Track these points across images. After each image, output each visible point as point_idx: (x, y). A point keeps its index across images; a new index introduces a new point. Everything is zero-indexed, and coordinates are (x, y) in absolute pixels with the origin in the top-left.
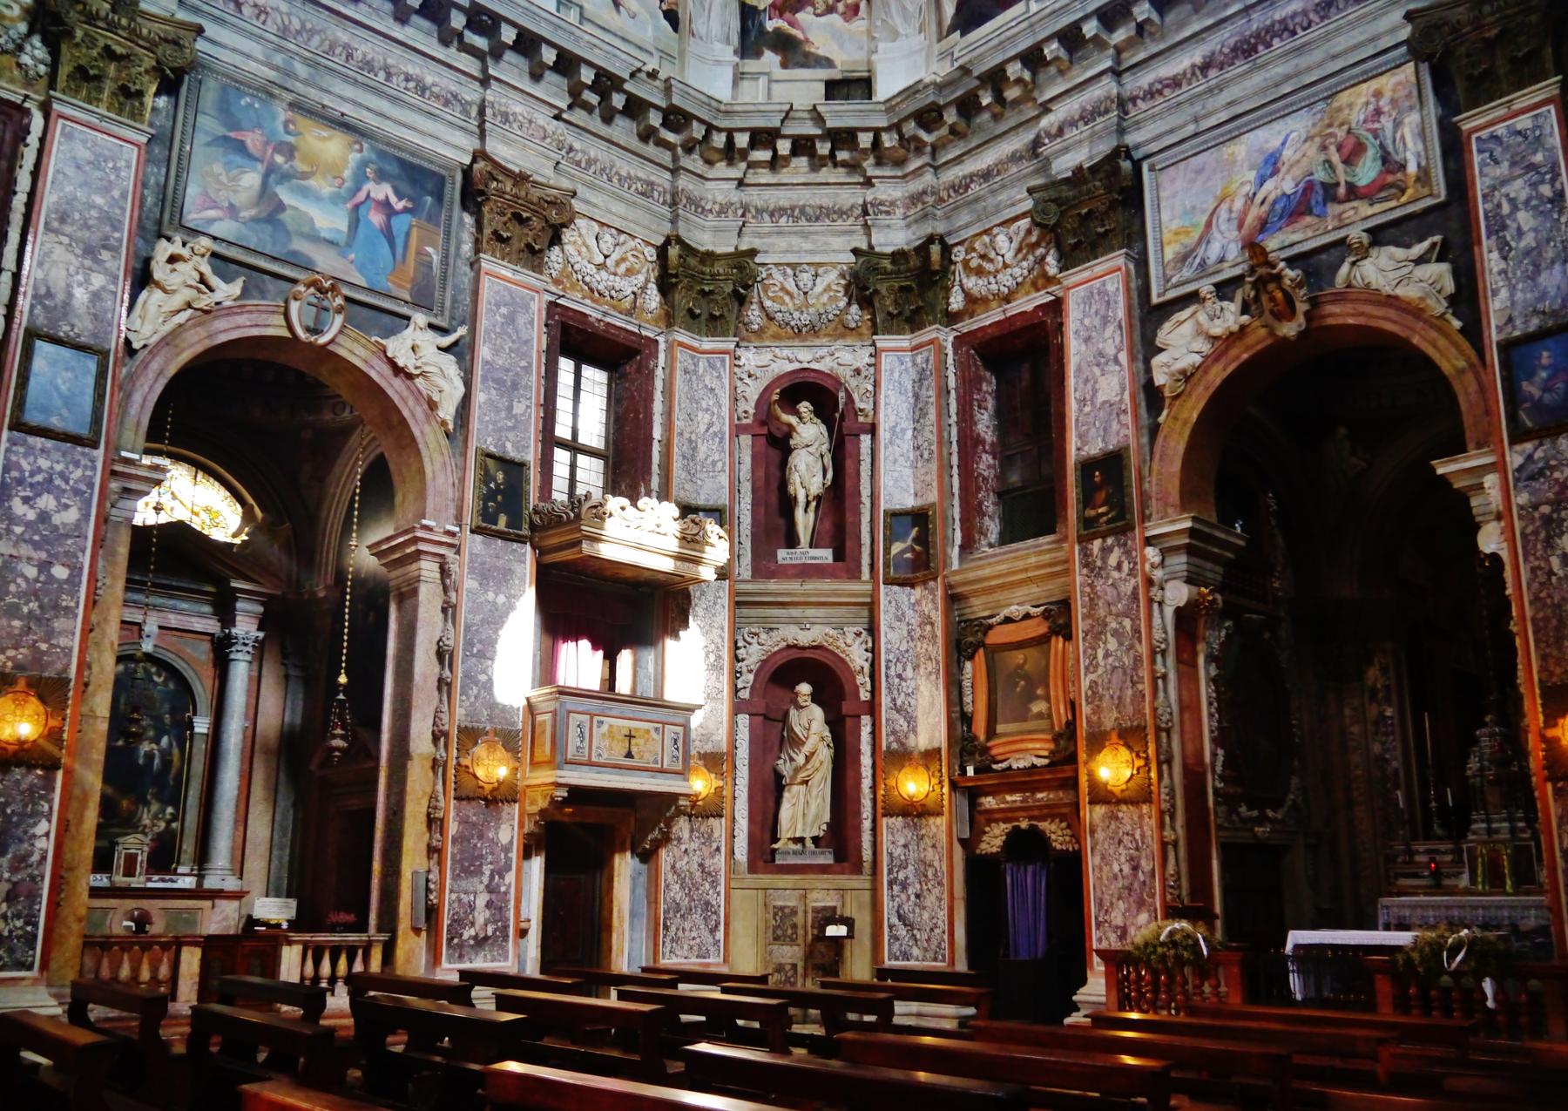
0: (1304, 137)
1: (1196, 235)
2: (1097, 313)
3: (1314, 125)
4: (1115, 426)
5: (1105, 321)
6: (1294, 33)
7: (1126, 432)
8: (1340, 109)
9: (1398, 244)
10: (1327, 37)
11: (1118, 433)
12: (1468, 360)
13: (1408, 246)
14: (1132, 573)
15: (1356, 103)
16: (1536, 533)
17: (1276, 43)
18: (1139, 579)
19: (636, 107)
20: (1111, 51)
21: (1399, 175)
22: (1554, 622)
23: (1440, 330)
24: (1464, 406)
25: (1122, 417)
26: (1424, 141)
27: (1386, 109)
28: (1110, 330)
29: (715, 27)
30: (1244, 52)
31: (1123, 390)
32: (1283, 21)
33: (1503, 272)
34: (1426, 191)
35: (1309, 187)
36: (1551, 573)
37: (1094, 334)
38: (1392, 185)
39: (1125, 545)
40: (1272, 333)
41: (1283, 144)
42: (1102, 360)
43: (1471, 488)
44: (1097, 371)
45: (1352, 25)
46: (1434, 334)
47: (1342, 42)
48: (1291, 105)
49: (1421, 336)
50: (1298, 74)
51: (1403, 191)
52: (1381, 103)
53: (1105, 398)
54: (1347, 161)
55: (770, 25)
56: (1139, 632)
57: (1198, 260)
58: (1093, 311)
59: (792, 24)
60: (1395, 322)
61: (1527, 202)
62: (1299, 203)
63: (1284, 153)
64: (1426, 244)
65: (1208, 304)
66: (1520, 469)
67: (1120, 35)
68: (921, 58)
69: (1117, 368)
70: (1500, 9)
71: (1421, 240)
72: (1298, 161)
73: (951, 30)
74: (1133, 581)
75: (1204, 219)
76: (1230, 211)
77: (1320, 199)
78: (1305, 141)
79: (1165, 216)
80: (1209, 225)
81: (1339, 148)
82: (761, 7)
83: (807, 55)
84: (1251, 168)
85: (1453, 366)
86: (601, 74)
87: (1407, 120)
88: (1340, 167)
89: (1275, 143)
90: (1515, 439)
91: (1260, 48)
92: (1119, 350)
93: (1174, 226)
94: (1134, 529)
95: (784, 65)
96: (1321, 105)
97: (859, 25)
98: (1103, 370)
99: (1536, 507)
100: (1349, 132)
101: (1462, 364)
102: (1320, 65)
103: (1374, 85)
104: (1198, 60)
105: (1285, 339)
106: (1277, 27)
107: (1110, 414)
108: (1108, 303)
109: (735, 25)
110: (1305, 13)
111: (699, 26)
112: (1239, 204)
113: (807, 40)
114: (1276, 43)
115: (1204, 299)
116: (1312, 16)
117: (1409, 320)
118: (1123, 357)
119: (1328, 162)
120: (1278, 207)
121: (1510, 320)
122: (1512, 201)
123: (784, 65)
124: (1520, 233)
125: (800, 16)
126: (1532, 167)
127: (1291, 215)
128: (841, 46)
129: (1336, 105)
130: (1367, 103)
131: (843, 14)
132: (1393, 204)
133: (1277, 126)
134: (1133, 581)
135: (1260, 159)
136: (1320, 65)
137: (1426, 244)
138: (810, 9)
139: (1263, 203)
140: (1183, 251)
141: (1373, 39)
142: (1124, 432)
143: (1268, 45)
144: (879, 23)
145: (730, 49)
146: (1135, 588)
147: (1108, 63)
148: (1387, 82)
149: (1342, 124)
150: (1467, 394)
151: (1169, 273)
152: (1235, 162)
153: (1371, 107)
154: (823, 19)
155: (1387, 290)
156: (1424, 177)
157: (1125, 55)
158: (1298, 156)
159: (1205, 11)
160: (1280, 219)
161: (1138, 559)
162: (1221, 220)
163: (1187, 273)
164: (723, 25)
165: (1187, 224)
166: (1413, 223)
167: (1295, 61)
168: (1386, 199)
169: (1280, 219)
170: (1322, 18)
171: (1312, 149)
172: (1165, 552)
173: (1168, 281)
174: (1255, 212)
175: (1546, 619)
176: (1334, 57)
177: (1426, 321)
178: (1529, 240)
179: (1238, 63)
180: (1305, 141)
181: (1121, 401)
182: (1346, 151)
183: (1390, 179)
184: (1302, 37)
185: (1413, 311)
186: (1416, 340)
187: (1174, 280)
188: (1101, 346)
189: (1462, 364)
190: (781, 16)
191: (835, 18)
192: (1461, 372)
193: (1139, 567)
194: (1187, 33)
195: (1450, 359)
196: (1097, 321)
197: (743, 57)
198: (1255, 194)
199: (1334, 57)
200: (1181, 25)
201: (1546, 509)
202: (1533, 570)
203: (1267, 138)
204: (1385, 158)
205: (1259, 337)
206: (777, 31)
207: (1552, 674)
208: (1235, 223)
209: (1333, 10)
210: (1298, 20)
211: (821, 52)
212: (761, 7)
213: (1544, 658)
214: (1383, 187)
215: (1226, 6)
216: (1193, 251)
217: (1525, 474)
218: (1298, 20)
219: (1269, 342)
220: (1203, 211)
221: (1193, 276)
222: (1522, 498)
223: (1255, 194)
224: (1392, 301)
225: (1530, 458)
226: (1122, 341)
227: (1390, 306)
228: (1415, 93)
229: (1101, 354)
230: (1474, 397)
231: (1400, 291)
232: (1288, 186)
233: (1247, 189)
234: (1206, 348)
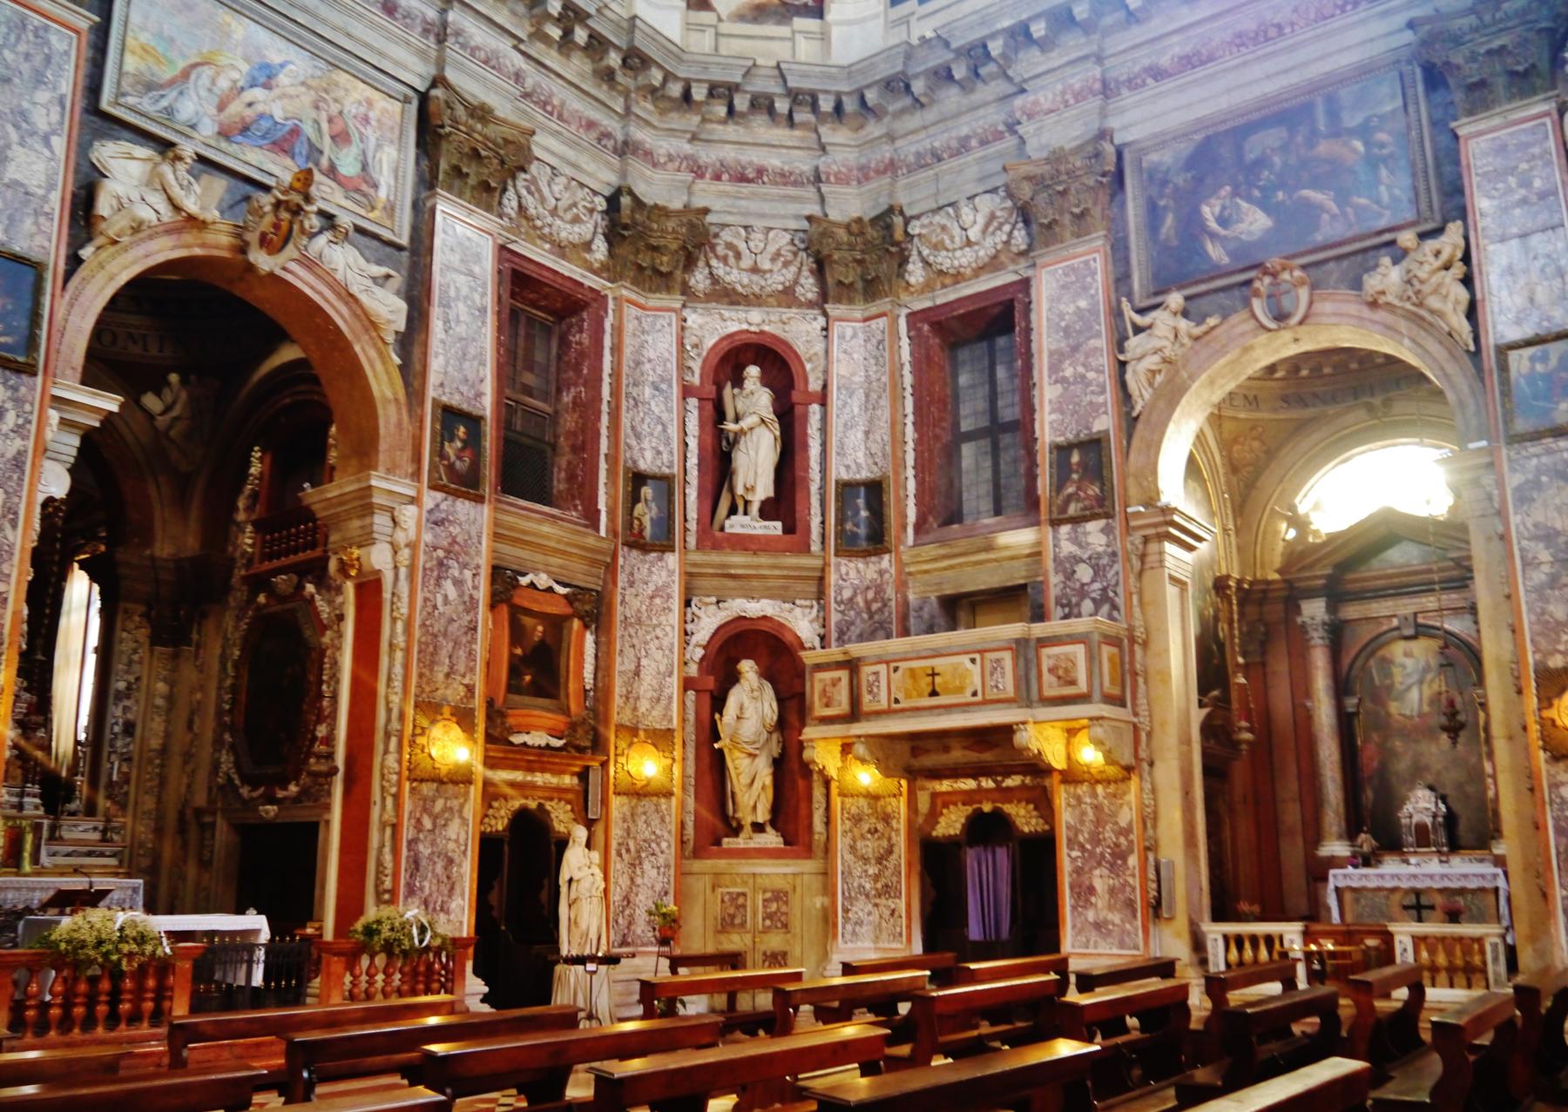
0: (302, 79)
1: (167, 74)
2: (27, 56)
3: (313, 77)
4: (28, 225)
5: (39, 80)
7: (46, 244)
8: (337, 85)
9: (362, 254)
11: (32, 236)
12: (395, 394)
13: (368, 261)
14: (19, 430)
15: (354, 95)
16: (431, 570)
18: (31, 444)
21: (371, 191)
22: (431, 648)
23: (380, 353)
24: (382, 431)
25: (42, 220)
26: (396, 178)
27: (373, 123)
28: (43, 96)
31: (51, 187)
33: (443, 342)
34: (388, 223)
35: (295, 132)
36: (435, 607)
37: (16, 81)
38: (365, 195)
39: (15, 389)
40: (243, 249)
41: (282, 66)
42: (24, 125)
43: (382, 508)
44: (14, 136)
46: (373, 353)
48: (300, 37)
49: (363, 349)
50: (315, 16)
51: (373, 208)
52: (371, 115)
53: (18, 177)
54: (333, 138)
56: (16, 513)
57: (164, 103)
58: (22, 48)
60: (345, 321)
61: (466, 298)
62: (284, 139)
63: (281, 76)
64: (383, 270)
65: (181, 166)
66: (430, 512)
69: (47, 153)
70: (485, 137)
71: (379, 263)
72: (291, 97)
74: (18, 443)
75: (182, 64)
76: (213, 82)
77: (304, 152)
78: (303, 84)
79: (135, 18)
80: (185, 74)
81: (330, 121)
84: (247, 59)
85: (382, 391)
87: (386, 149)
88: (327, 140)
89: (275, 58)
90: (434, 487)
92: (54, 132)
93: (144, 37)
94: (34, 374)
96: (322, 64)
98: (22, 137)
99: (435, 549)
100: (341, 113)
101: (389, 394)
102: (335, 28)
103: (370, 92)
105: (251, 268)
107: (26, 204)
108: (48, 59)
112: (224, 84)
115: (179, 158)
117: (357, 326)
118: (59, 143)
119: (316, 122)
120: (265, 124)
121: (442, 385)
122: (457, 289)
124: (458, 321)
126: (471, 274)
127: (274, 143)
129: (334, 76)
130: (360, 103)
132: (362, 212)
133: (282, 44)
134: (18, 443)
135: (257, 60)
136: (335, 28)
137: (383, 270)
139: (250, 105)
140: (148, 77)
141: (381, 54)
142: (40, 240)
146: (21, 454)
148: (381, 102)
149: (336, 100)
150: (387, 422)
151: (126, 87)
152: (229, 36)
153: (362, 110)
155: (354, 290)
156: (390, 209)
158: (291, 91)
160: (263, 137)
161: (34, 418)
162: (200, 83)
163: (146, 104)
165: (160, 49)
166: (375, 243)
168: (357, 203)
169: (263, 137)
171: (307, 98)
172: (64, 422)
173: (124, 95)
174: (236, 108)
175: (427, 644)
176: (349, 35)
177: (371, 338)
178: (461, 330)
180: (303, 84)
181: (45, 199)
182: (338, 127)
183: (364, 187)
185: (370, 324)
186: (357, 348)
187: (131, 100)
188: (25, 105)
189: (389, 394)
192: (386, 400)
193: (33, 428)
195: (383, 380)
196: (25, 67)
198: (242, 89)
199: (349, 35)
201: (441, 553)
202: (426, 600)
203: (276, 50)
204: (364, 167)
205: (219, 241)
207: (423, 691)
208: (216, 100)
213: (421, 675)
214: (357, 190)
216: (161, 87)
217: (433, 518)
219: (225, 254)
220: (184, 56)
221: (154, 115)
222: (427, 537)
223: (242, 89)
224: (350, 299)
225: (437, 506)
226: (61, 123)
227: (346, 303)
228: (397, 131)
229: (23, 114)
230: (392, 428)
231: (363, 298)
232: (279, 115)
233: (235, 75)
234: (167, 214)
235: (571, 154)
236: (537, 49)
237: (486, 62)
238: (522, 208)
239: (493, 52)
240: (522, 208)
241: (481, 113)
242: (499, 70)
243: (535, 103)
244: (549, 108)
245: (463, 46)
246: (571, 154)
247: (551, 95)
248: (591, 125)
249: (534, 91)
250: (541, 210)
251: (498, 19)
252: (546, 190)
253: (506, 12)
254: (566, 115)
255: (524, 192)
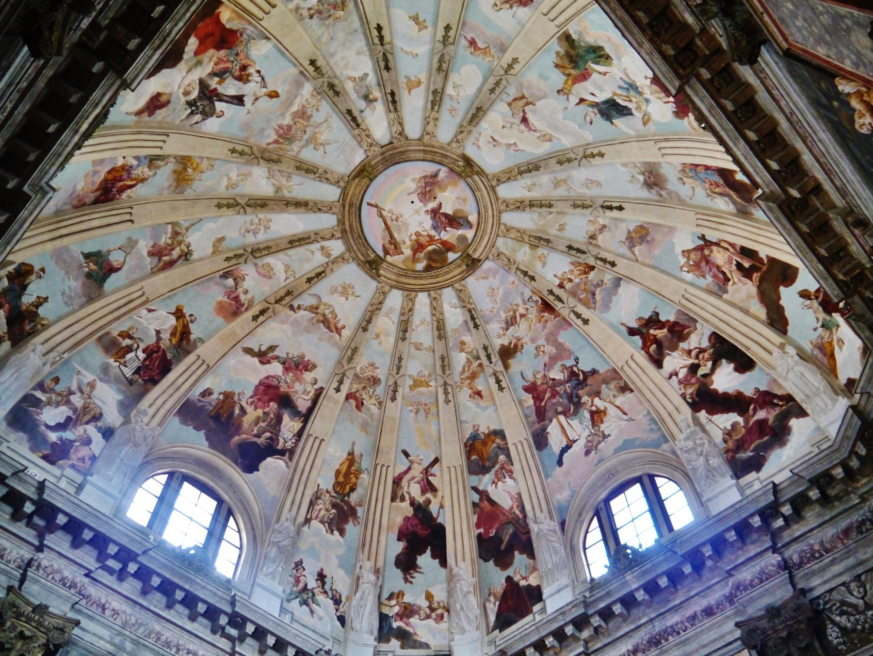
6: (679, 633)
10: (697, 636)
17: (670, 638)
19: (143, 574)
20: (582, 642)
29: (365, 624)
30: (654, 643)
32: (671, 627)
45: (709, 629)
47: (706, 638)
55: (395, 625)
59: (407, 624)
67: (586, 634)
68: (478, 644)
70: (783, 622)
73: (494, 629)
82: (391, 615)
83: (415, 641)
86: (122, 549)
91: (663, 641)
95: (402, 647)
97: (444, 625)
104: (630, 647)
106: (669, 630)
109: (376, 624)
110: (682, 622)
111: (356, 625)
113: (415, 634)
114: (670, 638)
116: (687, 624)
123: (402, 647)
125: (411, 620)
128: (434, 637)
131: (435, 619)
138: (417, 616)
141: (722, 637)
143: (667, 640)
144: (454, 625)
145: (373, 638)
147: (581, 649)
154: (424, 622)
157: (590, 645)
159: (629, 621)
164: (370, 624)
167: (682, 649)
170: (692, 625)
176: (704, 646)
179: (652, 650)
184: (684, 636)
190: (401, 620)
191: (431, 622)
194: (621, 632)
197: (379, 642)
199: (704, 646)
200: (618, 628)
206: (399, 628)
209: (697, 621)
210: (679, 626)
211: (423, 640)
212: (391, 615)
215: (640, 618)
218: (679, 626)
235: (851, 561)
236: (786, 536)
237: (761, 581)
238: (843, 630)
239: (759, 574)
240: (843, 630)
241: (773, 612)
242: (771, 576)
243: (808, 562)
244: (817, 555)
245: (745, 589)
246: (851, 561)
247: (812, 546)
248: (846, 532)
249: (801, 558)
250: (852, 619)
251: (752, 554)
252: (853, 600)
253: (751, 547)
254: (828, 546)
255: (838, 619)
